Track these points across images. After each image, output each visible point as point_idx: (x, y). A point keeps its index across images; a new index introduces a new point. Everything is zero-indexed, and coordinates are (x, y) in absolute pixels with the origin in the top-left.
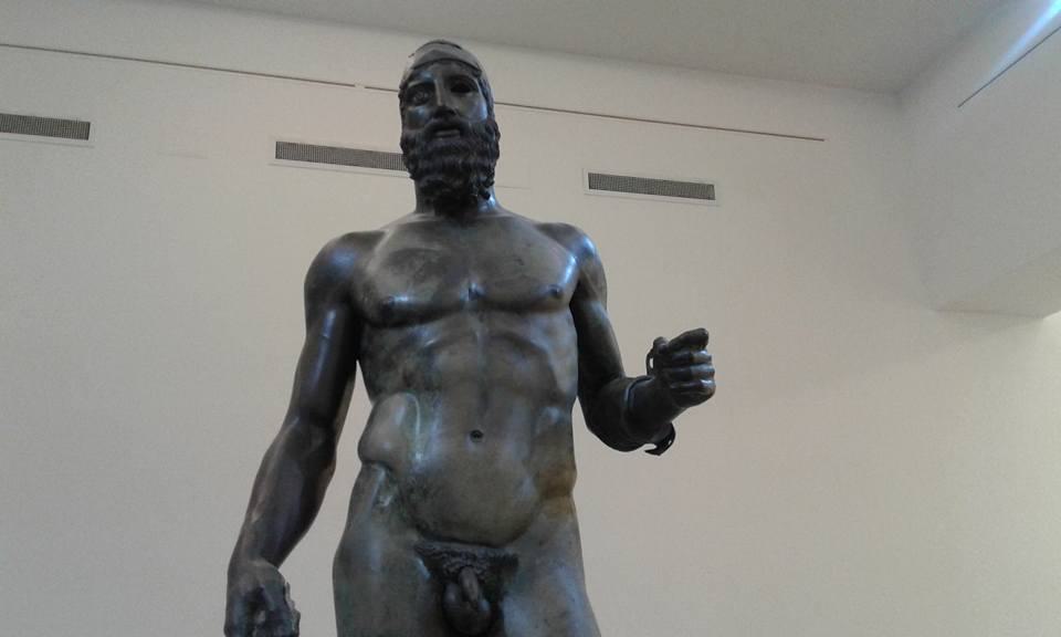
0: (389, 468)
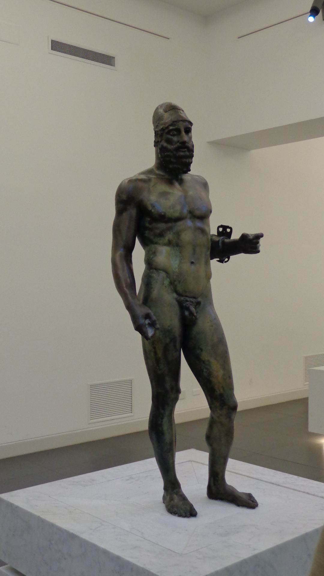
0: (166, 272)
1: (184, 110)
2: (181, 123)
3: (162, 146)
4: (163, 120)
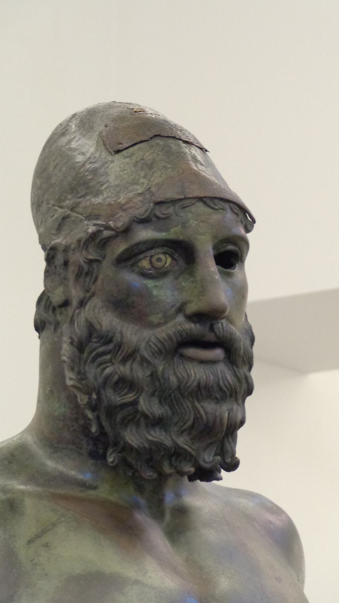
1: (206, 147)
2: (200, 208)
3: (91, 328)
4: (98, 193)
